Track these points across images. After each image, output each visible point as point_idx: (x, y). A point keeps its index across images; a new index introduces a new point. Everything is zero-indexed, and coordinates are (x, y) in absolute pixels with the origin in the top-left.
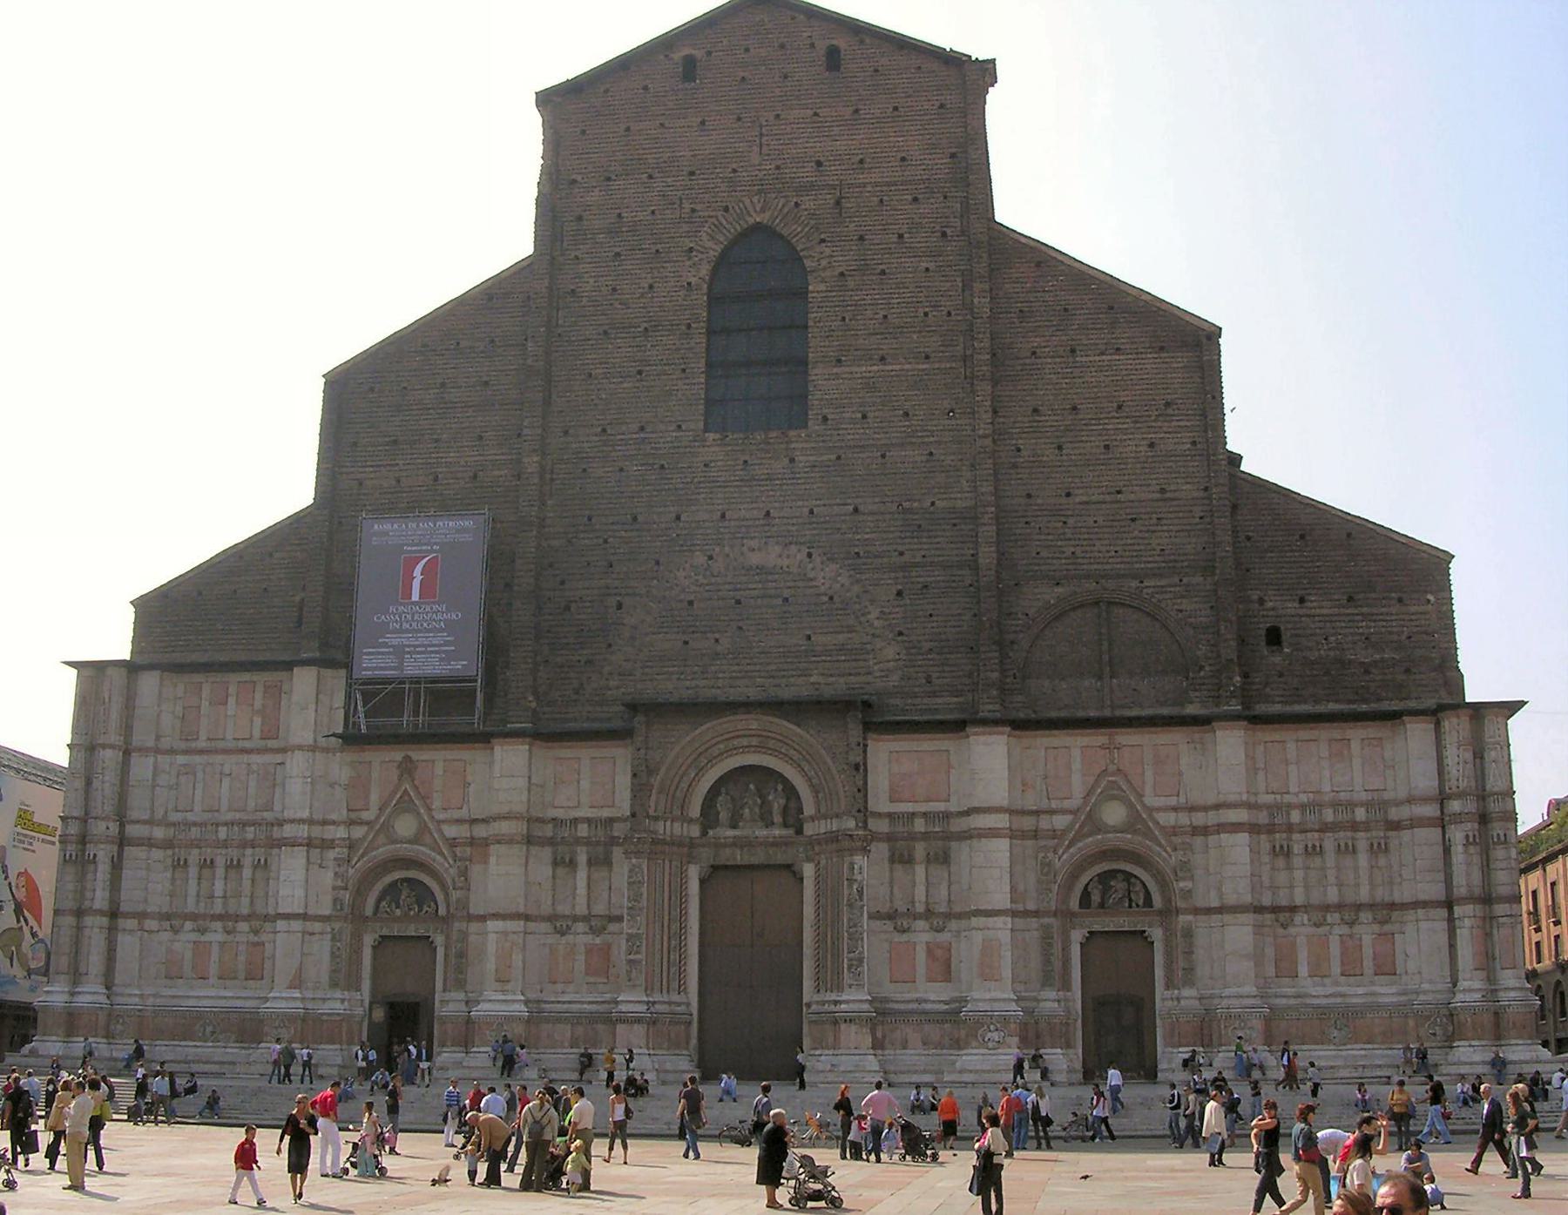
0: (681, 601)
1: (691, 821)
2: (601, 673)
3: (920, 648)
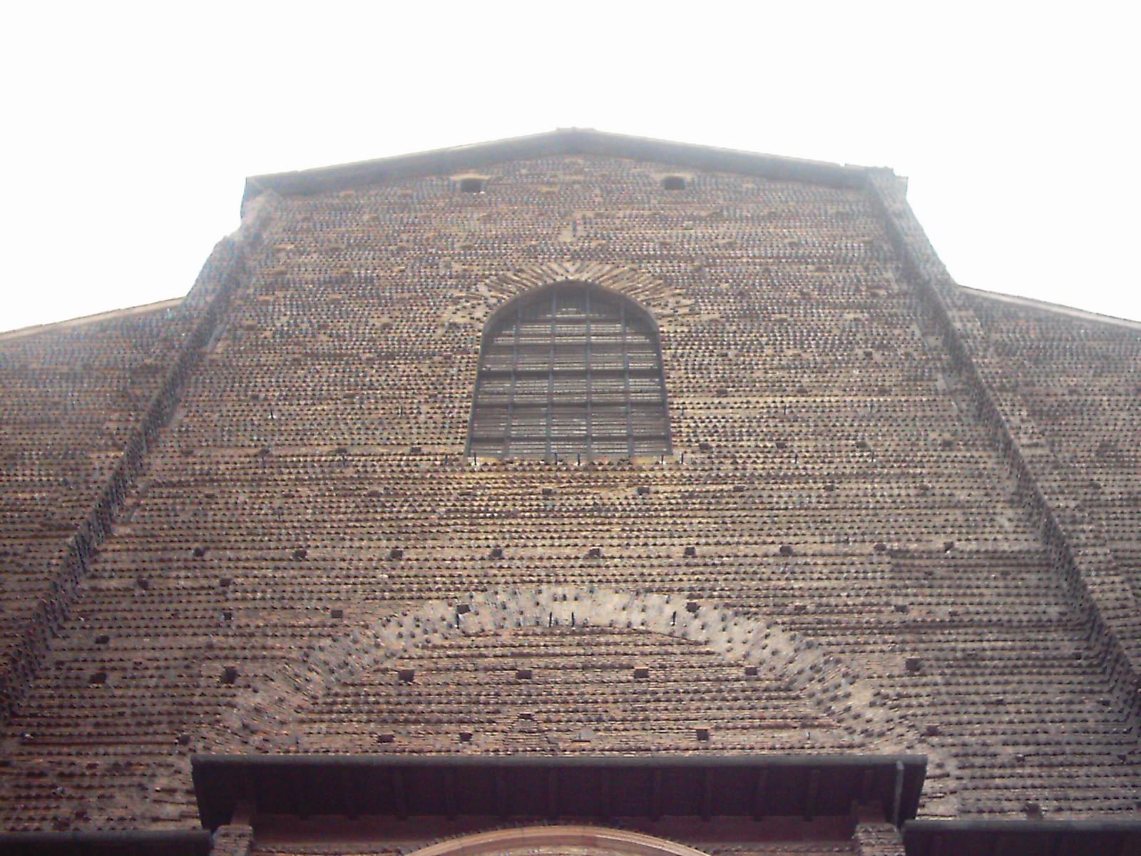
0: (385, 671)
2: (142, 787)
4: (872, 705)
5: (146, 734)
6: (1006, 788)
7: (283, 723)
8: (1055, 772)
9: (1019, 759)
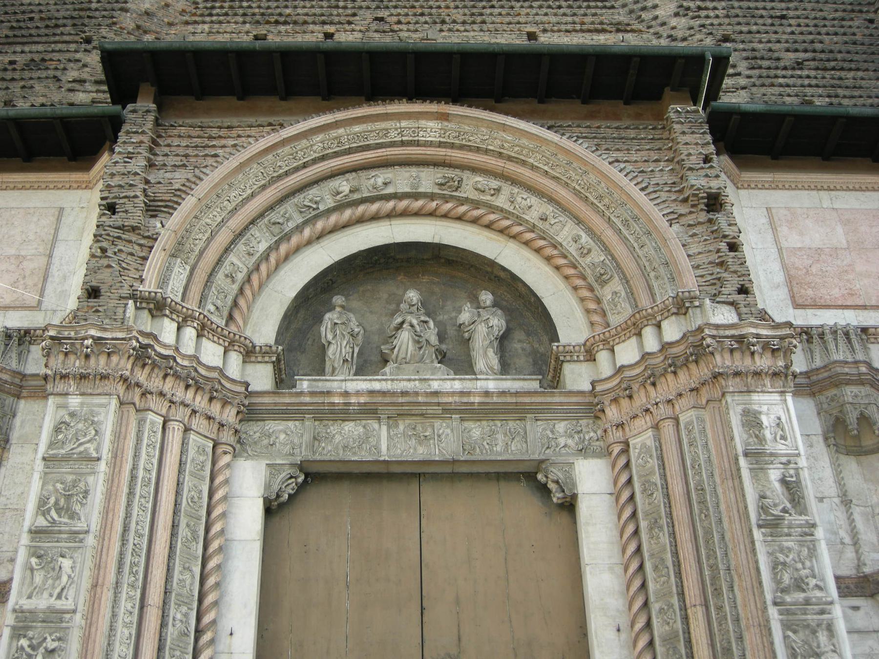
1: (250, 353)
3: (778, 59)
4: (677, 15)
5: (54, 35)
6: (788, 86)
7: (170, 24)
8: (828, 74)
9: (798, 63)
